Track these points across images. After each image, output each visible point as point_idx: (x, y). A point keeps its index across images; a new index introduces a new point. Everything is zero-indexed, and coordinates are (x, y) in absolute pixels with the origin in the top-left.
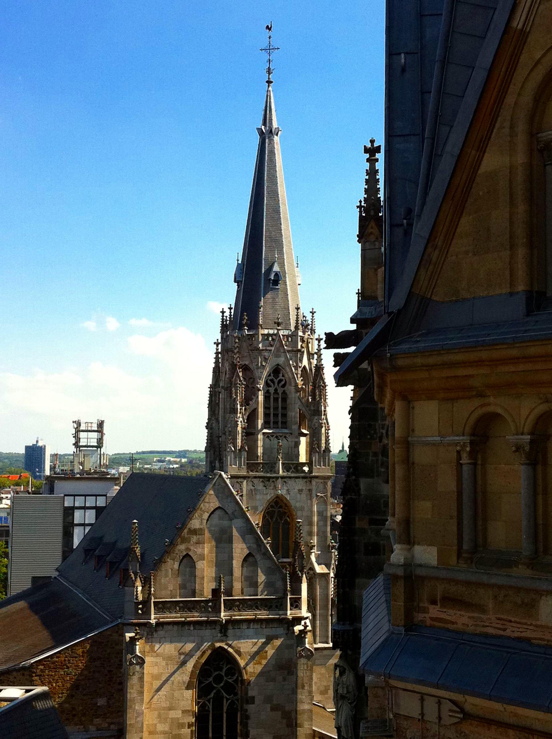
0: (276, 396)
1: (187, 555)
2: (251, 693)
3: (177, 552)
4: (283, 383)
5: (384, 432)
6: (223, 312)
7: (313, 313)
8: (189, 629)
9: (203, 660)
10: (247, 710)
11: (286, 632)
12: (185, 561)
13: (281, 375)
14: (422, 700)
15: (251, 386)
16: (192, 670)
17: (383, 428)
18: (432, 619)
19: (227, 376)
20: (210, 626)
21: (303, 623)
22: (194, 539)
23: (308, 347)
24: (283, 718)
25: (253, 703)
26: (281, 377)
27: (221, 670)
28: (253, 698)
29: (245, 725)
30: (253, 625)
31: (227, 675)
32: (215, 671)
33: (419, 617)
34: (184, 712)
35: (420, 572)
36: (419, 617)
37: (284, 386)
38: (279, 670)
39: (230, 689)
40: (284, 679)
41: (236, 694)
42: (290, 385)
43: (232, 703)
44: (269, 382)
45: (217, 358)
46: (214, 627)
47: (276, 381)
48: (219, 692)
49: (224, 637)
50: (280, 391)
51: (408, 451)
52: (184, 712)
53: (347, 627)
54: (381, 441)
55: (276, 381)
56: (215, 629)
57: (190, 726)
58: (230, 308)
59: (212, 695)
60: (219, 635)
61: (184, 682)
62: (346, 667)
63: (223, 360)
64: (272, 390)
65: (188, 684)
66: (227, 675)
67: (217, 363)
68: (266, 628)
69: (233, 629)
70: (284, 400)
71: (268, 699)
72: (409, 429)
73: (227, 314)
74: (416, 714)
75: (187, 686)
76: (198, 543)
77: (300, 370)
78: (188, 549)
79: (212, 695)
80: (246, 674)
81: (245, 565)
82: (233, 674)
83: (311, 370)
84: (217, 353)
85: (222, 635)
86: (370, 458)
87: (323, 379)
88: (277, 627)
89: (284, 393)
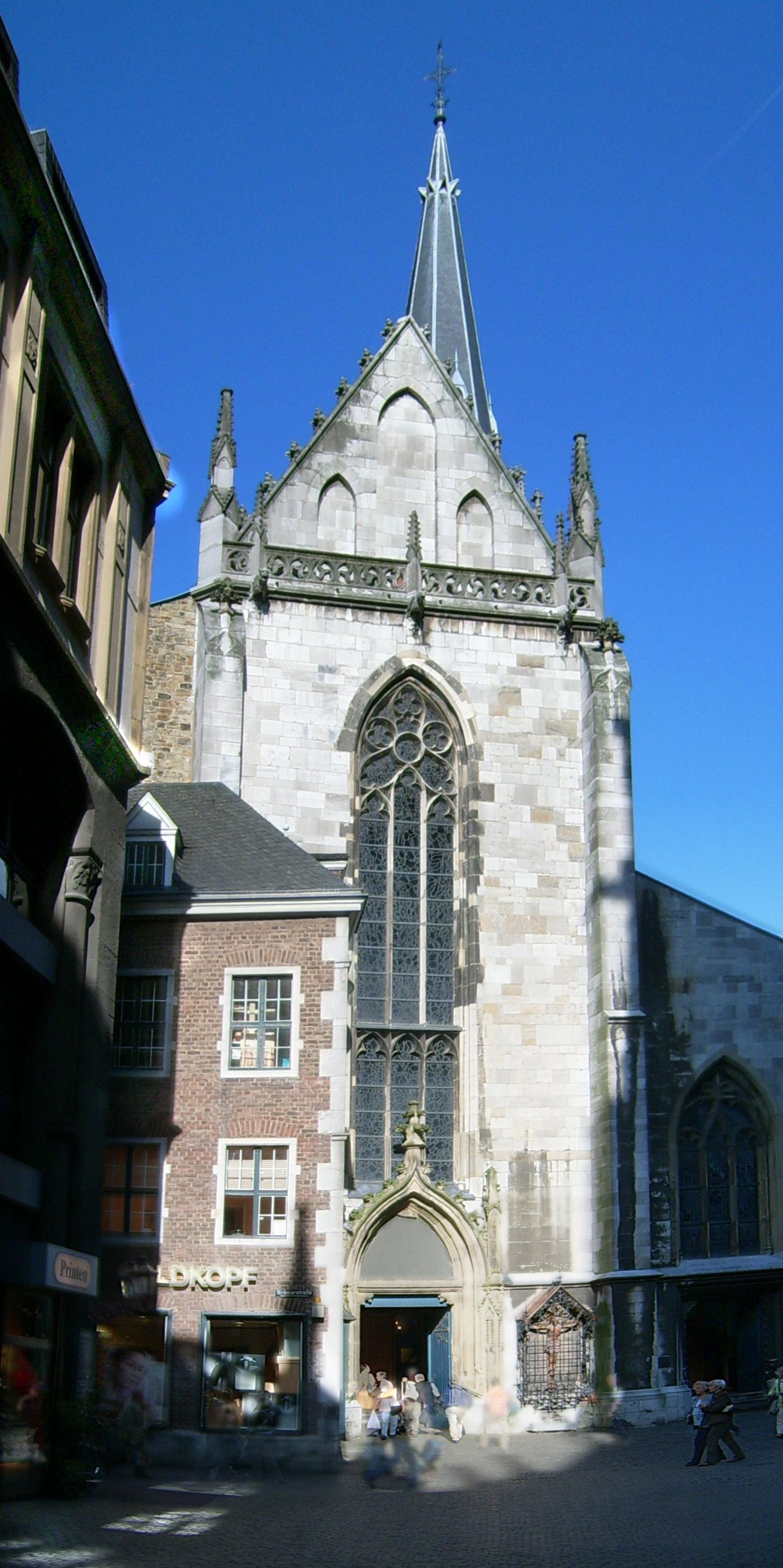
1: (337, 479)
8: (344, 619)
9: (373, 691)
10: (475, 813)
11: (561, 651)
12: (332, 492)
16: (350, 709)
20: (392, 619)
25: (491, 799)
28: (492, 786)
29: (472, 846)
30: (488, 628)
38: (548, 734)
40: (561, 755)
49: (423, 647)
56: (401, 625)
60: (412, 640)
65: (340, 737)
68: (516, 638)
69: (442, 631)
75: (338, 742)
78: (338, 463)
80: (474, 733)
81: (464, 520)
85: (418, 642)
88: (541, 641)
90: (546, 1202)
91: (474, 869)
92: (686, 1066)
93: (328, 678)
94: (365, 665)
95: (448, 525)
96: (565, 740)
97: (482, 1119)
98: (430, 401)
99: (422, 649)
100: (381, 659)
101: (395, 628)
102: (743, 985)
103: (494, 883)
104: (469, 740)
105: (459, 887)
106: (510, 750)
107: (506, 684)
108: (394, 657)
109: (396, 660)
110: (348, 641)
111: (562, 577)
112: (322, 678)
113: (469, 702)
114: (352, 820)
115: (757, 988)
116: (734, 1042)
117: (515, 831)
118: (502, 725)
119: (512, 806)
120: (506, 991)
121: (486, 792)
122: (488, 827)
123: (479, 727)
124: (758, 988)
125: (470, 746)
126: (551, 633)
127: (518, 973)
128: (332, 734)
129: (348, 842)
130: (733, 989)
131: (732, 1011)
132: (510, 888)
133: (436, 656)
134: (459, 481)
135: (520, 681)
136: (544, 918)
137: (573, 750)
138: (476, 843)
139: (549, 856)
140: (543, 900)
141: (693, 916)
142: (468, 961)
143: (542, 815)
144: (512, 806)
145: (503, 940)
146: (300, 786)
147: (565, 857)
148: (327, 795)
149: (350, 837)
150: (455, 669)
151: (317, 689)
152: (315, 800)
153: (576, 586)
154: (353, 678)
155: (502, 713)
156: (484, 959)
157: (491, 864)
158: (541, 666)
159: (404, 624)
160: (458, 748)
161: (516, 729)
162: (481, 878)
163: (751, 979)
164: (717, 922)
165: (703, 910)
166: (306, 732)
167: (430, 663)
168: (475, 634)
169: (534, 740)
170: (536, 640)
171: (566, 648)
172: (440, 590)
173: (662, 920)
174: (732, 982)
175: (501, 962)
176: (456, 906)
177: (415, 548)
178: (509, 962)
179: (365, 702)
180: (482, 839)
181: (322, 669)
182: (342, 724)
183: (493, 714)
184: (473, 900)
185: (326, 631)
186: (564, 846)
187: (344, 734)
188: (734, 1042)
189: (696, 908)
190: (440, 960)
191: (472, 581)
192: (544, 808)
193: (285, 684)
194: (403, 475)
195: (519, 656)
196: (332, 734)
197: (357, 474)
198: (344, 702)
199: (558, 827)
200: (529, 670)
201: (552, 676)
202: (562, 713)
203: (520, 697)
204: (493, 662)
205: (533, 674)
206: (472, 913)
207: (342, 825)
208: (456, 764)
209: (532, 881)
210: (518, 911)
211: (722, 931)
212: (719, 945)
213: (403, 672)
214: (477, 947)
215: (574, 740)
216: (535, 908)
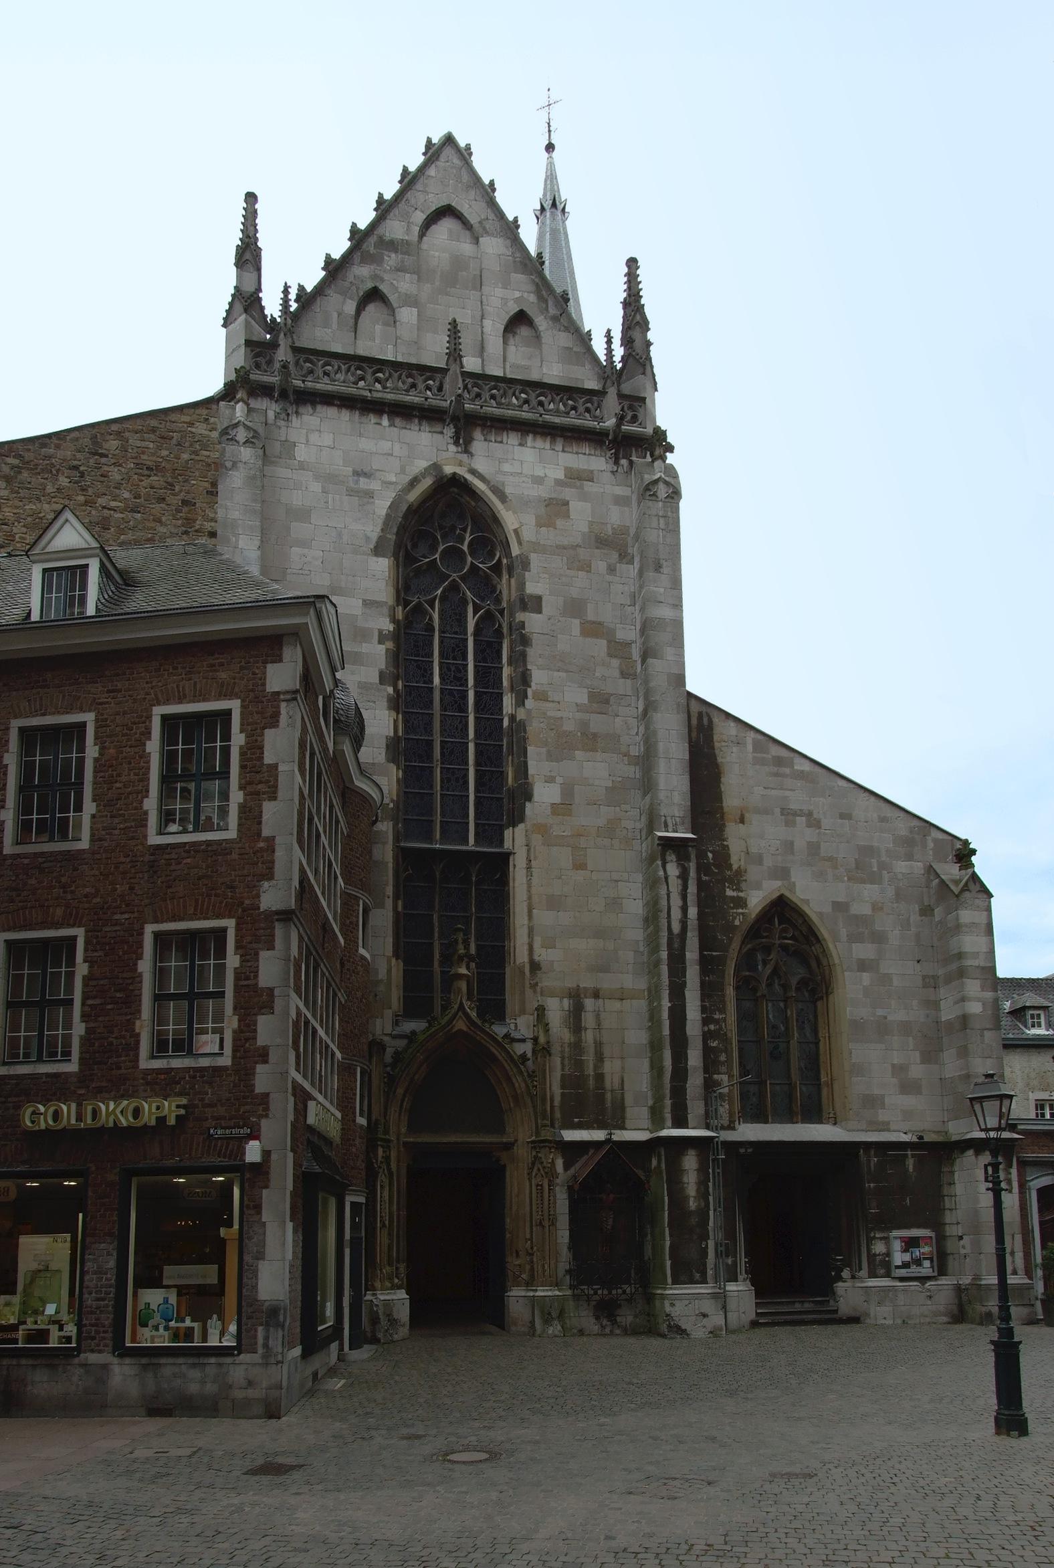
3: (351, 278)
8: (379, 424)
9: (413, 496)
10: (522, 625)
11: (610, 466)
16: (388, 515)
22: (392, 259)
24: (610, 655)
28: (539, 599)
29: (519, 659)
30: (534, 440)
34: (367, 603)
38: (597, 548)
40: (611, 570)
46: (439, 429)
48: (454, 587)
49: (466, 455)
52: (367, 603)
56: (442, 433)
57: (382, 639)
60: (452, 448)
65: (377, 542)
68: (563, 451)
69: (485, 440)
71: (575, 608)
75: (375, 547)
80: (520, 543)
85: (460, 450)
88: (589, 454)
93: (363, 483)
94: (403, 471)
96: (615, 556)
99: (464, 457)
100: (422, 464)
101: (435, 435)
102: (801, 821)
103: (542, 697)
104: (515, 550)
105: (508, 702)
107: (553, 496)
108: (435, 464)
109: (436, 467)
110: (385, 446)
111: (612, 392)
112: (357, 482)
113: (515, 512)
114: (391, 627)
115: (814, 823)
116: (793, 880)
118: (548, 537)
119: (560, 619)
122: (536, 640)
124: (817, 824)
125: (517, 556)
126: (601, 447)
127: (568, 791)
128: (367, 538)
129: (387, 650)
130: (789, 823)
131: (789, 846)
132: (559, 702)
133: (481, 464)
135: (568, 493)
136: (595, 736)
137: (624, 566)
138: (524, 655)
141: (749, 741)
142: (515, 778)
143: (593, 629)
144: (560, 619)
145: (550, 757)
147: (617, 673)
148: (364, 601)
149: (390, 645)
150: (500, 478)
151: (352, 492)
153: (626, 404)
154: (391, 483)
156: (533, 776)
157: (539, 677)
158: (591, 480)
159: (445, 431)
160: (505, 561)
162: (530, 692)
163: (810, 814)
164: (775, 751)
165: (759, 737)
166: (340, 535)
167: (473, 472)
168: (520, 445)
169: (583, 553)
170: (585, 454)
171: (616, 462)
172: (483, 400)
173: (717, 745)
174: (789, 815)
175: (550, 780)
176: (506, 723)
177: (455, 354)
178: (559, 780)
179: (404, 508)
180: (531, 652)
181: (358, 474)
182: (378, 529)
183: (539, 525)
184: (521, 715)
185: (360, 435)
186: (615, 663)
188: (793, 880)
189: (752, 734)
190: (490, 780)
191: (517, 393)
192: (594, 622)
193: (316, 487)
194: (447, 294)
195: (566, 469)
197: (397, 288)
198: (382, 506)
199: (609, 642)
200: (578, 483)
201: (602, 490)
202: (613, 529)
203: (569, 510)
204: (539, 472)
205: (581, 487)
206: (519, 727)
207: (380, 631)
208: (505, 576)
209: (582, 697)
210: (569, 726)
211: (779, 761)
212: (777, 775)
213: (445, 480)
214: (526, 763)
215: (625, 556)
216: (584, 725)
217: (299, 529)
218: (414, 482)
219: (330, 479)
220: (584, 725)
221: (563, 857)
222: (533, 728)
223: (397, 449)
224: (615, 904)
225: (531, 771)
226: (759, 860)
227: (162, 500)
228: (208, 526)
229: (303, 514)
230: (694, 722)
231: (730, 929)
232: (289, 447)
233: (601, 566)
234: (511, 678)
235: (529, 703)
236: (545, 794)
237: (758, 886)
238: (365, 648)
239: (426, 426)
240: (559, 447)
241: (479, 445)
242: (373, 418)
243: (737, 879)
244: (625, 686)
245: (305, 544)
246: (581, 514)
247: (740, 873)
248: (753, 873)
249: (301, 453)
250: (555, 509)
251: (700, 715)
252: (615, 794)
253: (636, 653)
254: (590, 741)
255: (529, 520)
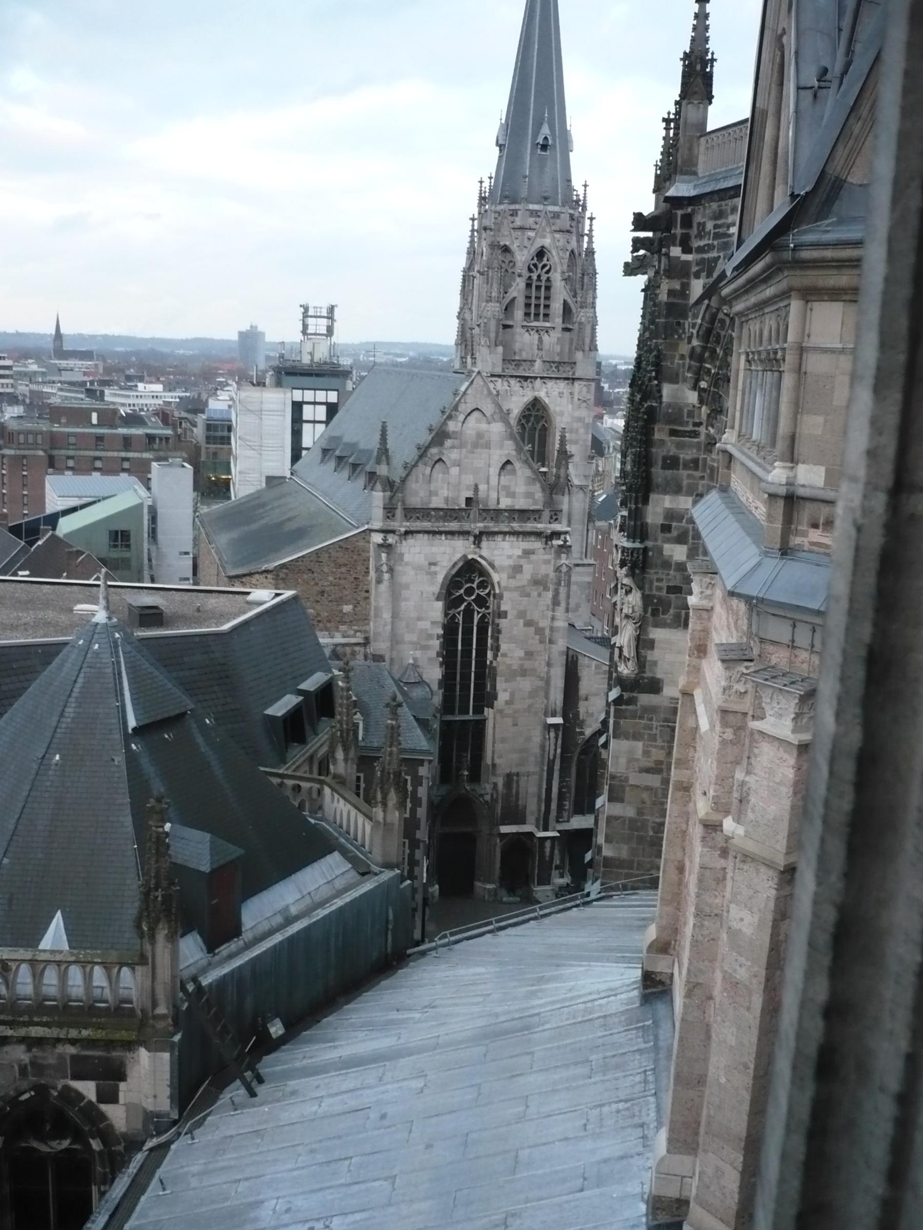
0: (538, 283)
1: (440, 460)
2: (503, 608)
3: (429, 455)
4: (547, 268)
5: (695, 332)
6: (481, 182)
7: (585, 186)
9: (453, 572)
10: (498, 625)
12: (437, 466)
13: (545, 259)
14: (794, 626)
15: (510, 271)
17: (693, 327)
18: (813, 544)
19: (484, 258)
21: (562, 537)
23: (578, 227)
24: (536, 634)
25: (506, 617)
26: (545, 261)
27: (473, 582)
28: (506, 612)
29: (496, 639)
31: (478, 588)
32: (467, 582)
33: (796, 541)
34: (433, 623)
35: (801, 492)
36: (796, 541)
37: (548, 272)
39: (481, 602)
40: (539, 595)
41: (488, 608)
42: (556, 271)
43: (484, 616)
44: (532, 267)
45: (472, 236)
47: (540, 266)
50: (544, 278)
51: (801, 358)
52: (433, 623)
53: (637, 545)
54: (689, 342)
55: (540, 266)
58: (490, 178)
59: (462, 607)
60: (473, 546)
61: (434, 594)
62: (633, 586)
63: (480, 238)
64: (535, 277)
66: (478, 588)
67: (472, 242)
70: (548, 288)
71: (522, 614)
72: (804, 332)
73: (486, 184)
74: (786, 638)
76: (453, 447)
77: (568, 254)
78: (441, 453)
79: (462, 607)
82: (486, 588)
83: (580, 255)
84: (473, 231)
86: (676, 361)
87: (593, 266)
89: (548, 280)
90: (517, 793)
91: (496, 649)
92: (582, 733)
93: (433, 568)
95: (494, 481)
96: (542, 588)
97: (493, 759)
98: (488, 414)
99: (477, 550)
100: (458, 556)
103: (505, 655)
104: (497, 591)
106: (516, 595)
109: (465, 556)
110: (442, 549)
117: (515, 632)
118: (513, 583)
120: (507, 703)
121: (503, 615)
123: (502, 585)
127: (512, 694)
133: (484, 553)
134: (501, 456)
135: (523, 562)
139: (530, 641)
140: (527, 662)
143: (528, 624)
145: (506, 681)
146: (419, 619)
149: (442, 640)
151: (428, 573)
152: (425, 625)
155: (514, 577)
157: (504, 647)
158: (533, 553)
161: (520, 584)
167: (481, 557)
171: (546, 544)
175: (505, 690)
179: (450, 577)
181: (431, 564)
183: (509, 577)
186: (537, 637)
187: (439, 593)
194: (473, 453)
196: (434, 594)
198: (440, 578)
204: (510, 552)
206: (494, 670)
209: (521, 653)
210: (515, 667)
217: (405, 593)
218: (455, 564)
219: (418, 568)
220: (522, 665)
221: (509, 721)
222: (501, 669)
223: (448, 550)
224: (529, 739)
225: (498, 688)
226: (592, 715)
227: (345, 579)
228: (365, 588)
229: (407, 587)
230: (570, 659)
231: (577, 744)
232: (402, 555)
233: (535, 594)
234: (492, 645)
235: (499, 659)
236: (503, 697)
237: (590, 726)
238: (431, 642)
239: (461, 537)
240: (520, 539)
241: (484, 544)
242: (438, 536)
243: (581, 724)
244: (540, 647)
245: (406, 600)
246: (528, 569)
247: (583, 721)
248: (589, 721)
249: (407, 558)
250: (517, 569)
251: (573, 656)
252: (533, 694)
253: (547, 632)
254: (524, 673)
255: (504, 576)
